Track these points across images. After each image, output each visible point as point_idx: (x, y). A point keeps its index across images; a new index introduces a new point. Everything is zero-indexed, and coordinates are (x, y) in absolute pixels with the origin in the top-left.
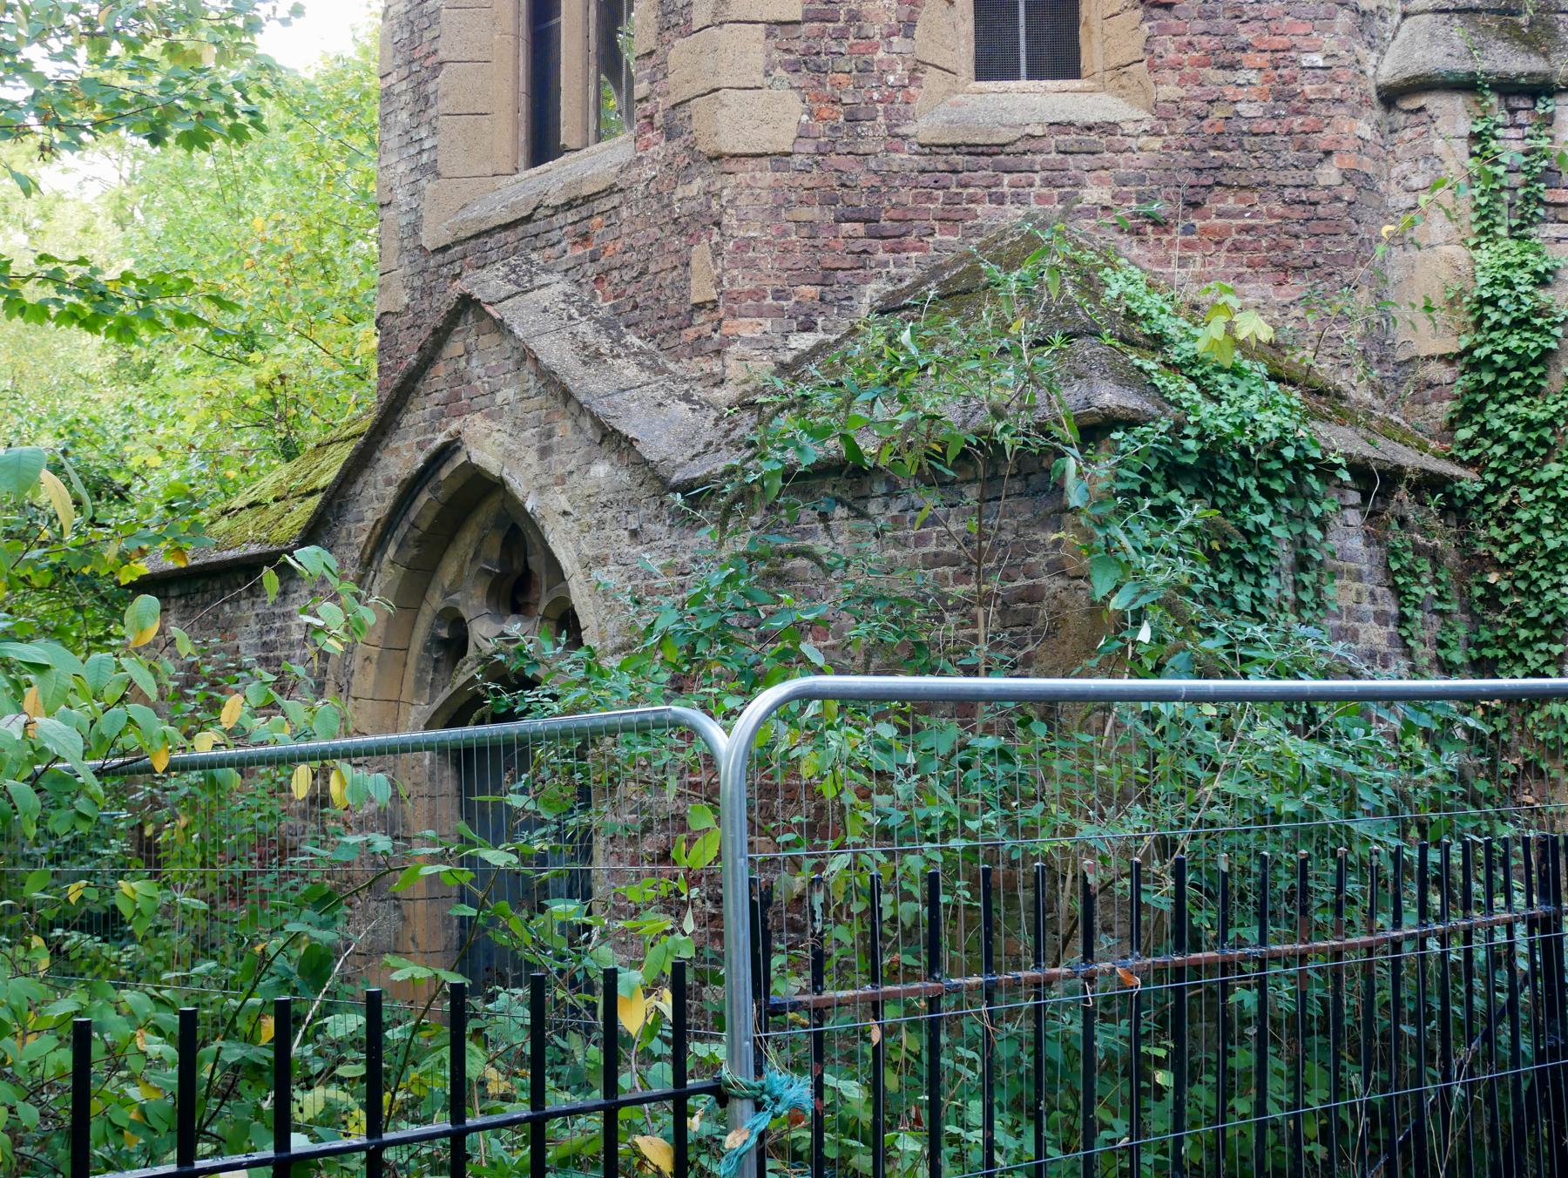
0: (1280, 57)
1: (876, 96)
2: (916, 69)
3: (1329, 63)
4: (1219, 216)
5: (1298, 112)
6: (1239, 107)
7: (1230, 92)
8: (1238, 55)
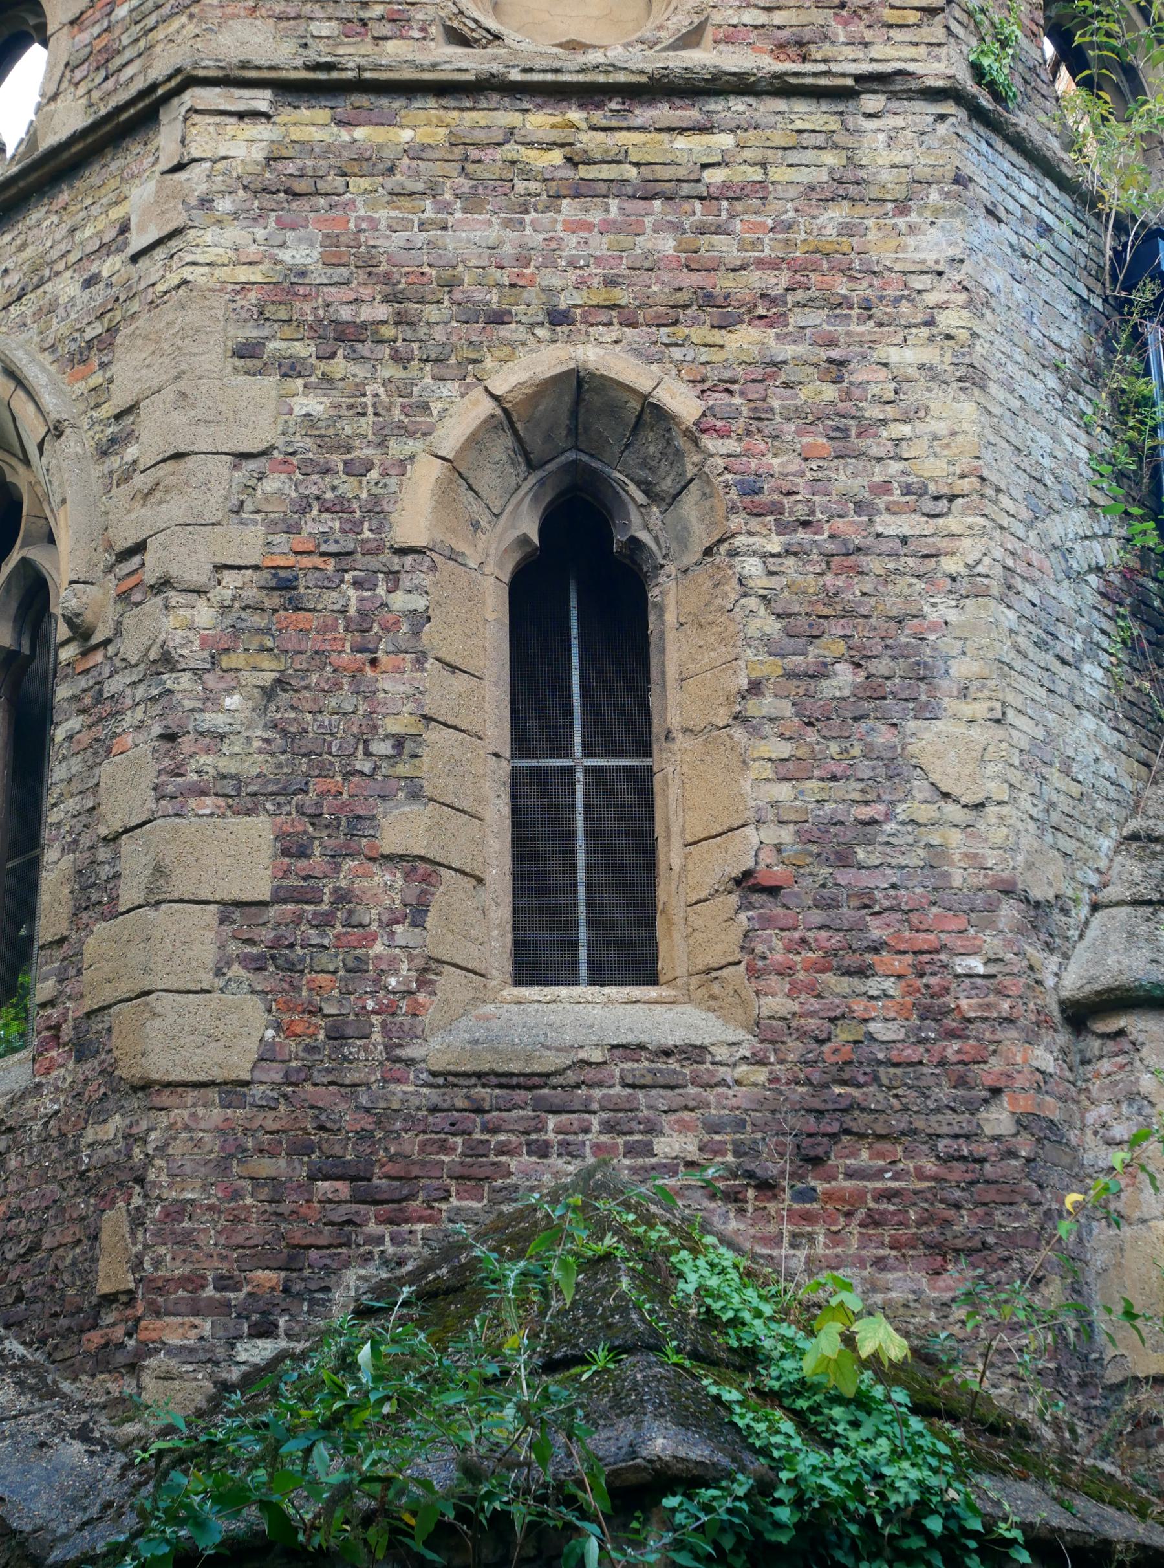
0: (927, 961)
1: (370, 1005)
2: (428, 969)
3: (992, 969)
4: (849, 1176)
5: (952, 1035)
6: (872, 1027)
7: (859, 1007)
8: (869, 958)
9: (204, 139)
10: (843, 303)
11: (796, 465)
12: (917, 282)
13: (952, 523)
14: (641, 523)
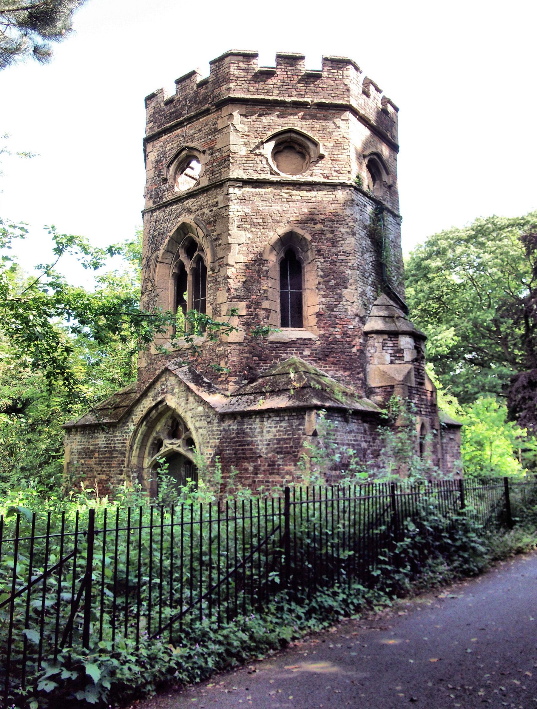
7: (334, 333)
9: (231, 190)
12: (346, 218)
13: (350, 258)
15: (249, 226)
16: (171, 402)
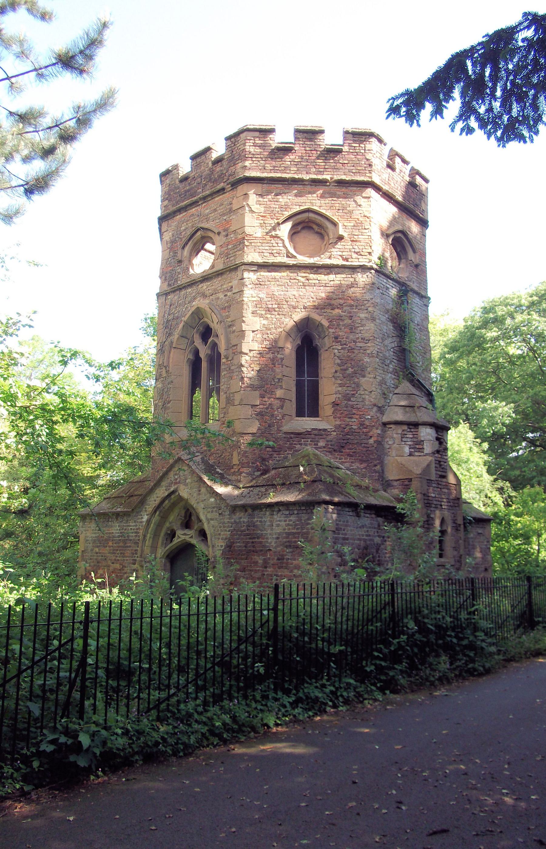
7: (350, 423)
9: (246, 275)
10: (353, 306)
11: (344, 334)
13: (369, 345)
14: (317, 342)
15: (263, 312)
16: (184, 492)
